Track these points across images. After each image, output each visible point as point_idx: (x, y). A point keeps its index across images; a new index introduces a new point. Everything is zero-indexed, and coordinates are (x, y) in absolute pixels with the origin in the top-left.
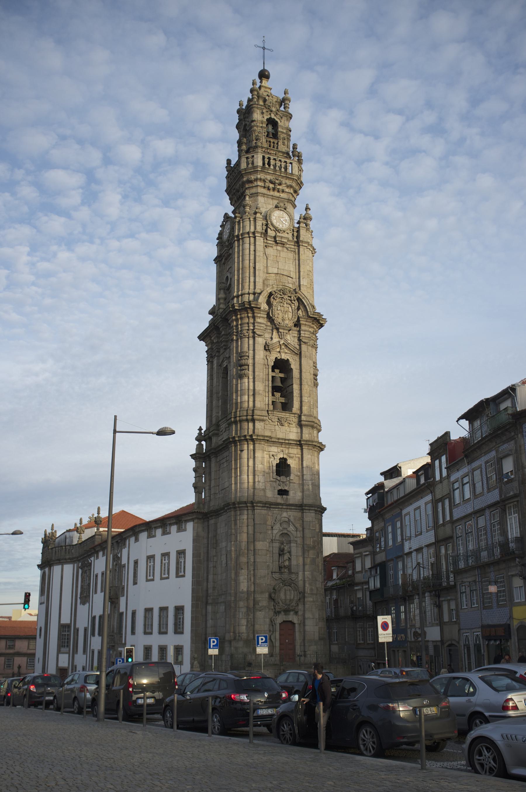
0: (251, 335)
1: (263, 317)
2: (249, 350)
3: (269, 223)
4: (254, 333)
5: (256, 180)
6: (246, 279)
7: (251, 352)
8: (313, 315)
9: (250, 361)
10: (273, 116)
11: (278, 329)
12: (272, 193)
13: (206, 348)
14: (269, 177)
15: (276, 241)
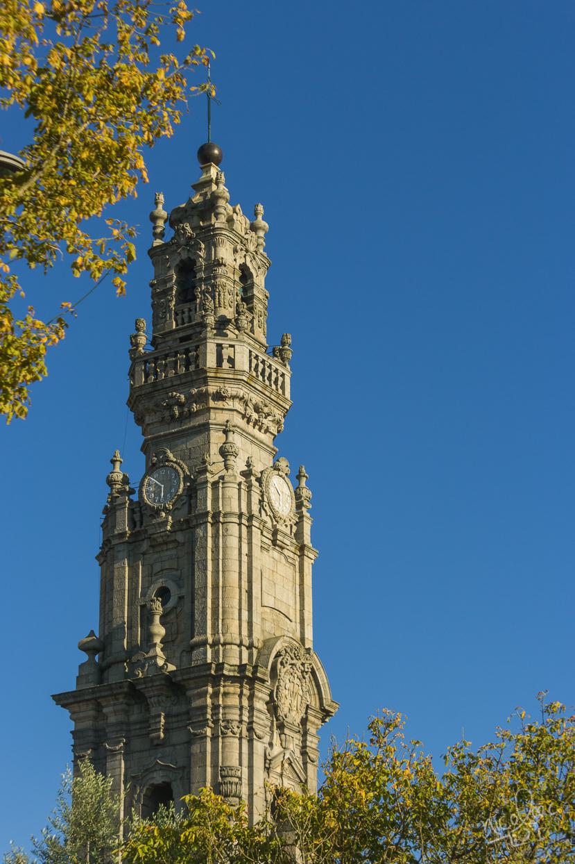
0: (245, 733)
1: (263, 700)
2: (240, 764)
3: (265, 499)
4: (250, 729)
5: (233, 397)
6: (232, 613)
7: (245, 770)
8: (329, 706)
9: (244, 790)
10: (249, 264)
11: (281, 727)
12: (250, 428)
13: (72, 726)
14: (256, 398)
15: (274, 542)
